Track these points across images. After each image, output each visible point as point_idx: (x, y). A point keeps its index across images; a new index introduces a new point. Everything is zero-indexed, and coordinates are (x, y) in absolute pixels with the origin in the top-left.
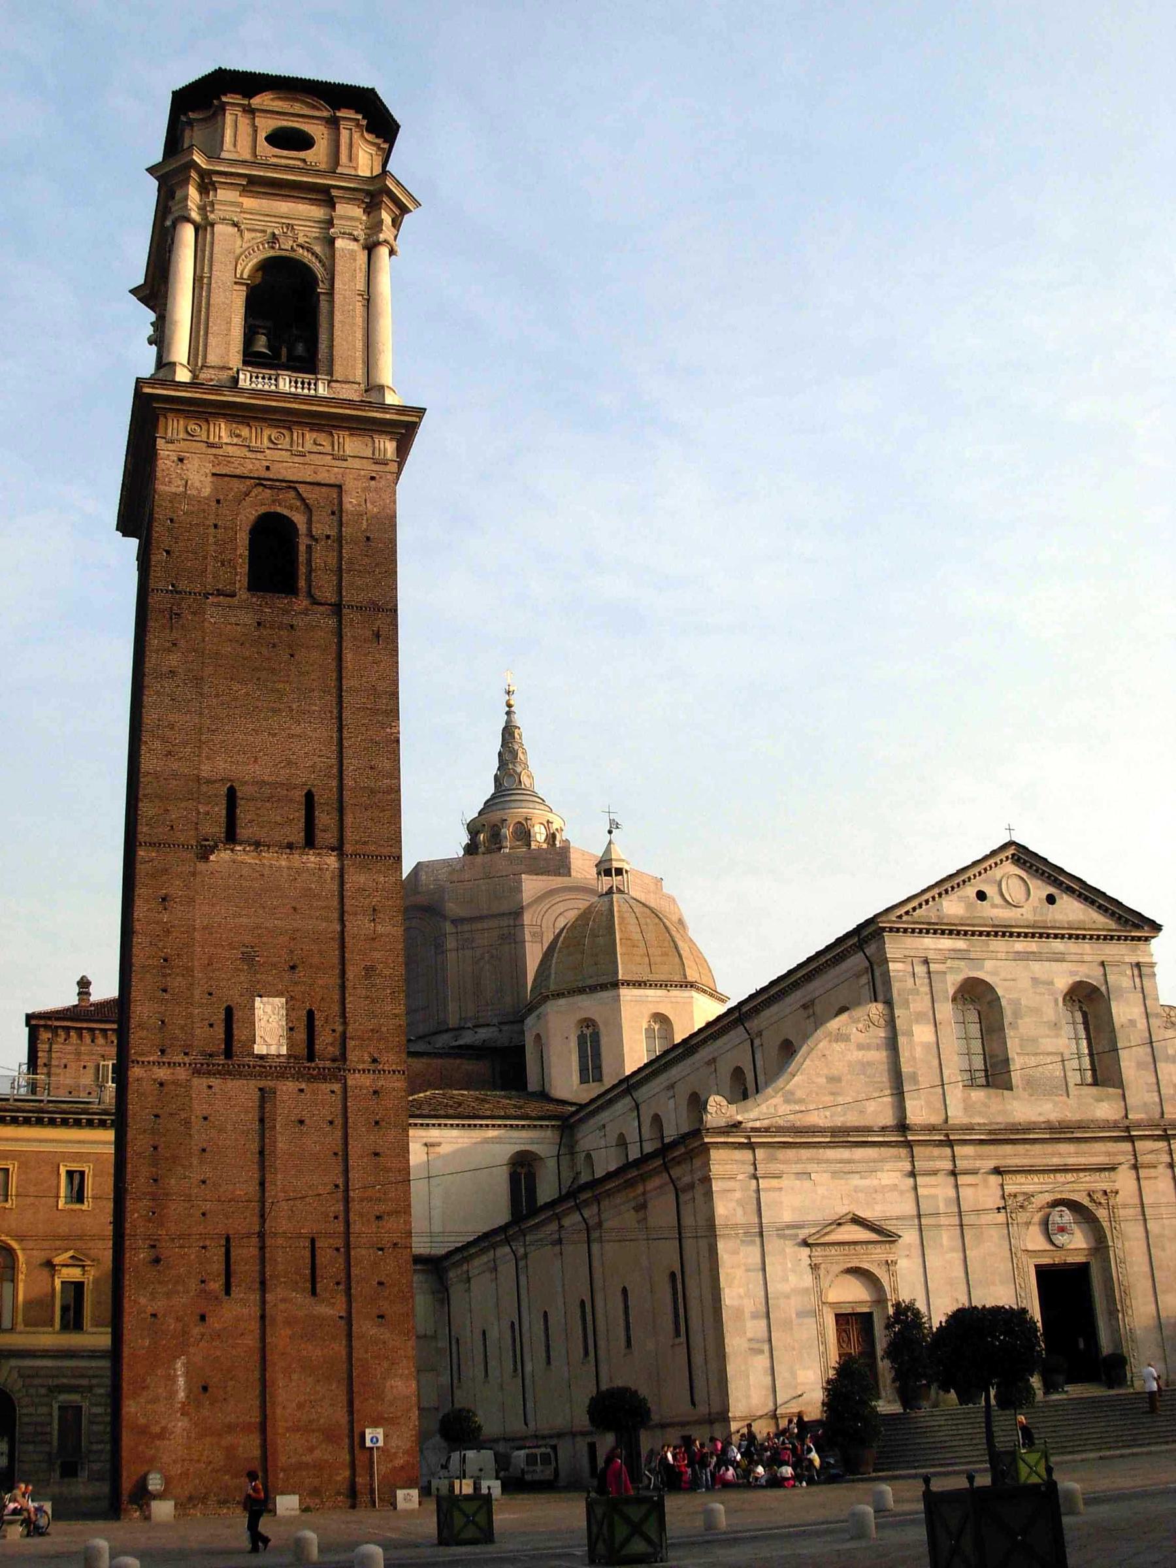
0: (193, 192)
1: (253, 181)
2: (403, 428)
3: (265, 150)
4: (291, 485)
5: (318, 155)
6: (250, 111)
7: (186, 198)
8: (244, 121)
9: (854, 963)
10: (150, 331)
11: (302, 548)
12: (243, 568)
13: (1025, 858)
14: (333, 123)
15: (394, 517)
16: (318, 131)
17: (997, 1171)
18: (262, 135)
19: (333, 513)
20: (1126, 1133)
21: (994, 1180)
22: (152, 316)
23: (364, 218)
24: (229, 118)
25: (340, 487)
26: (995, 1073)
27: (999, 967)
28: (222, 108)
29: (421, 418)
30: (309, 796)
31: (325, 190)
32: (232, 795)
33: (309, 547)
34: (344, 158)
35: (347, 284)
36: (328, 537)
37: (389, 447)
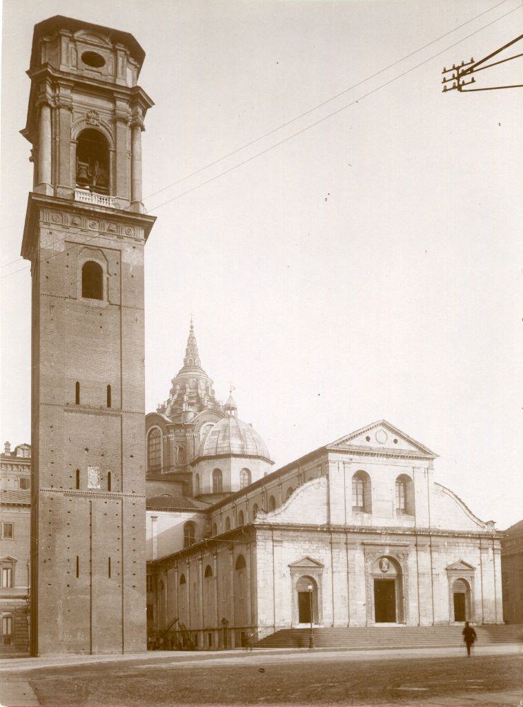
0: (49, 90)
1: (77, 84)
2: (146, 224)
3: (83, 65)
4: (99, 249)
5: (108, 69)
6: (73, 40)
7: (45, 92)
8: (71, 45)
9: (313, 465)
10: (30, 154)
11: (105, 278)
12: (79, 285)
13: (384, 424)
14: (114, 51)
15: (143, 267)
16: (105, 54)
17: (363, 544)
18: (80, 55)
19: (117, 263)
20: (415, 533)
21: (359, 547)
22: (31, 146)
23: (130, 110)
24: (64, 45)
25: (120, 251)
26: (365, 508)
27: (373, 467)
28: (60, 37)
29: (155, 220)
30: (109, 387)
31: (112, 92)
32: (78, 384)
33: (108, 279)
34: (119, 75)
35: (123, 145)
36: (115, 274)
37: (141, 234)
